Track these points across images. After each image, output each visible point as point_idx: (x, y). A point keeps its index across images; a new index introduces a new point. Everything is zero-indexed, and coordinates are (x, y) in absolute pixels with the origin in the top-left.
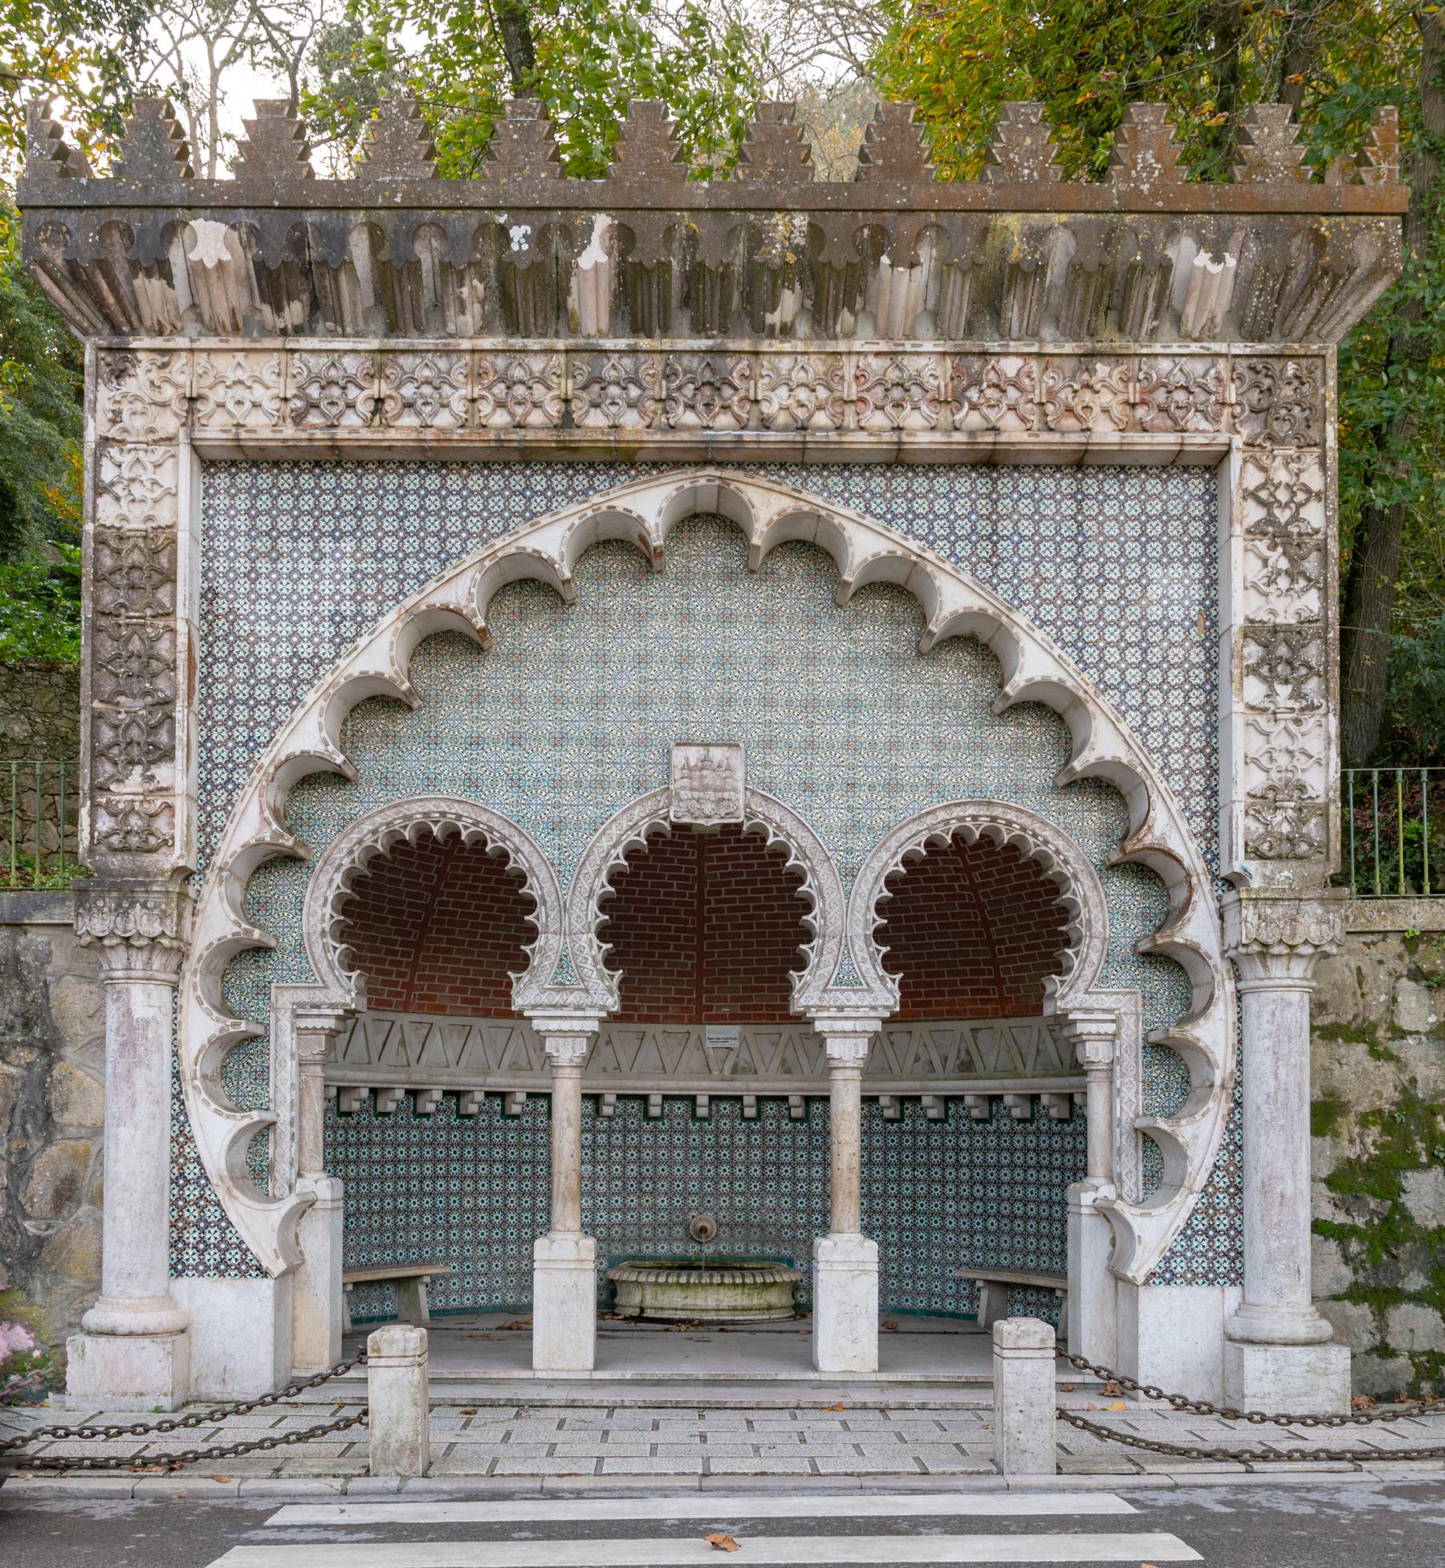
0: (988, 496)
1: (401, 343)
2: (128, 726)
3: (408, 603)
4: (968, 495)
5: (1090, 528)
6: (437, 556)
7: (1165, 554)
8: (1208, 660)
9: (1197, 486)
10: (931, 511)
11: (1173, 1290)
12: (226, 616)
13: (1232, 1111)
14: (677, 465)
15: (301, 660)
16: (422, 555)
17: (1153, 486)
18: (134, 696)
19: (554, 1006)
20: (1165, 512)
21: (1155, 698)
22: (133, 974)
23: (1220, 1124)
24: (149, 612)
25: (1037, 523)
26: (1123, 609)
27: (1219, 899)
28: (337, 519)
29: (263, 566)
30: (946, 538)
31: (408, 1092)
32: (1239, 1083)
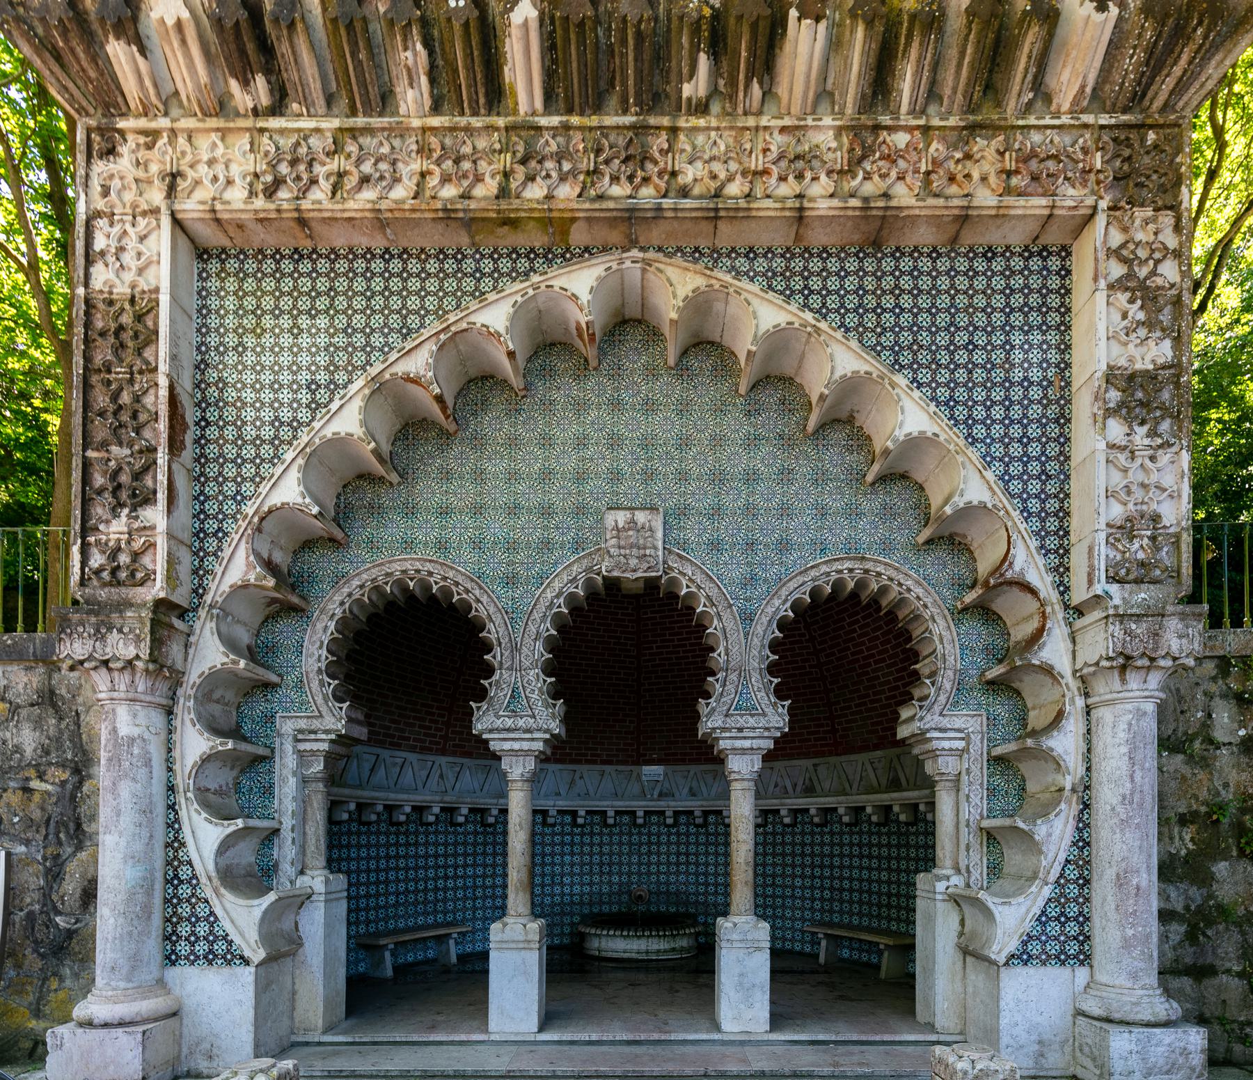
6: (400, 331)
16: (386, 330)
28: (313, 299)
29: (250, 341)
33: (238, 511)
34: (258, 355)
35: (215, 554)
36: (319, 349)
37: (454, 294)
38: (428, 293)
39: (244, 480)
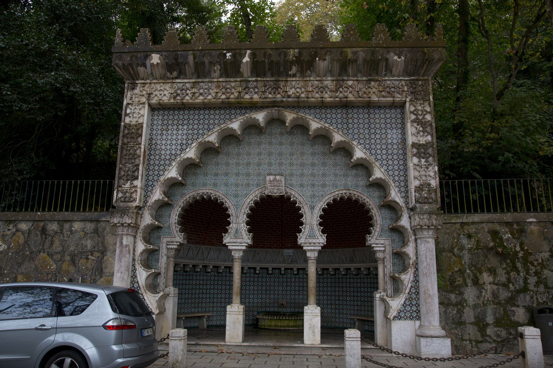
0: (346, 113)
1: (200, 80)
2: (128, 171)
3: (199, 140)
4: (340, 113)
5: (372, 121)
6: (207, 129)
7: (391, 127)
8: (404, 153)
9: (399, 111)
10: (331, 117)
11: (401, 322)
12: (154, 144)
13: (415, 271)
14: (267, 107)
15: (172, 155)
17: (388, 111)
18: (130, 164)
19: (234, 243)
20: (391, 117)
21: (390, 162)
22: (124, 233)
23: (412, 275)
24: (135, 143)
25: (358, 120)
26: (381, 140)
27: (409, 214)
28: (183, 121)
30: (335, 123)
31: (214, 267)
32: (417, 264)
33: (158, 179)
34: (167, 136)
35: (151, 191)
36: (184, 134)
37: (223, 119)
38: (216, 119)
39: (160, 170)
